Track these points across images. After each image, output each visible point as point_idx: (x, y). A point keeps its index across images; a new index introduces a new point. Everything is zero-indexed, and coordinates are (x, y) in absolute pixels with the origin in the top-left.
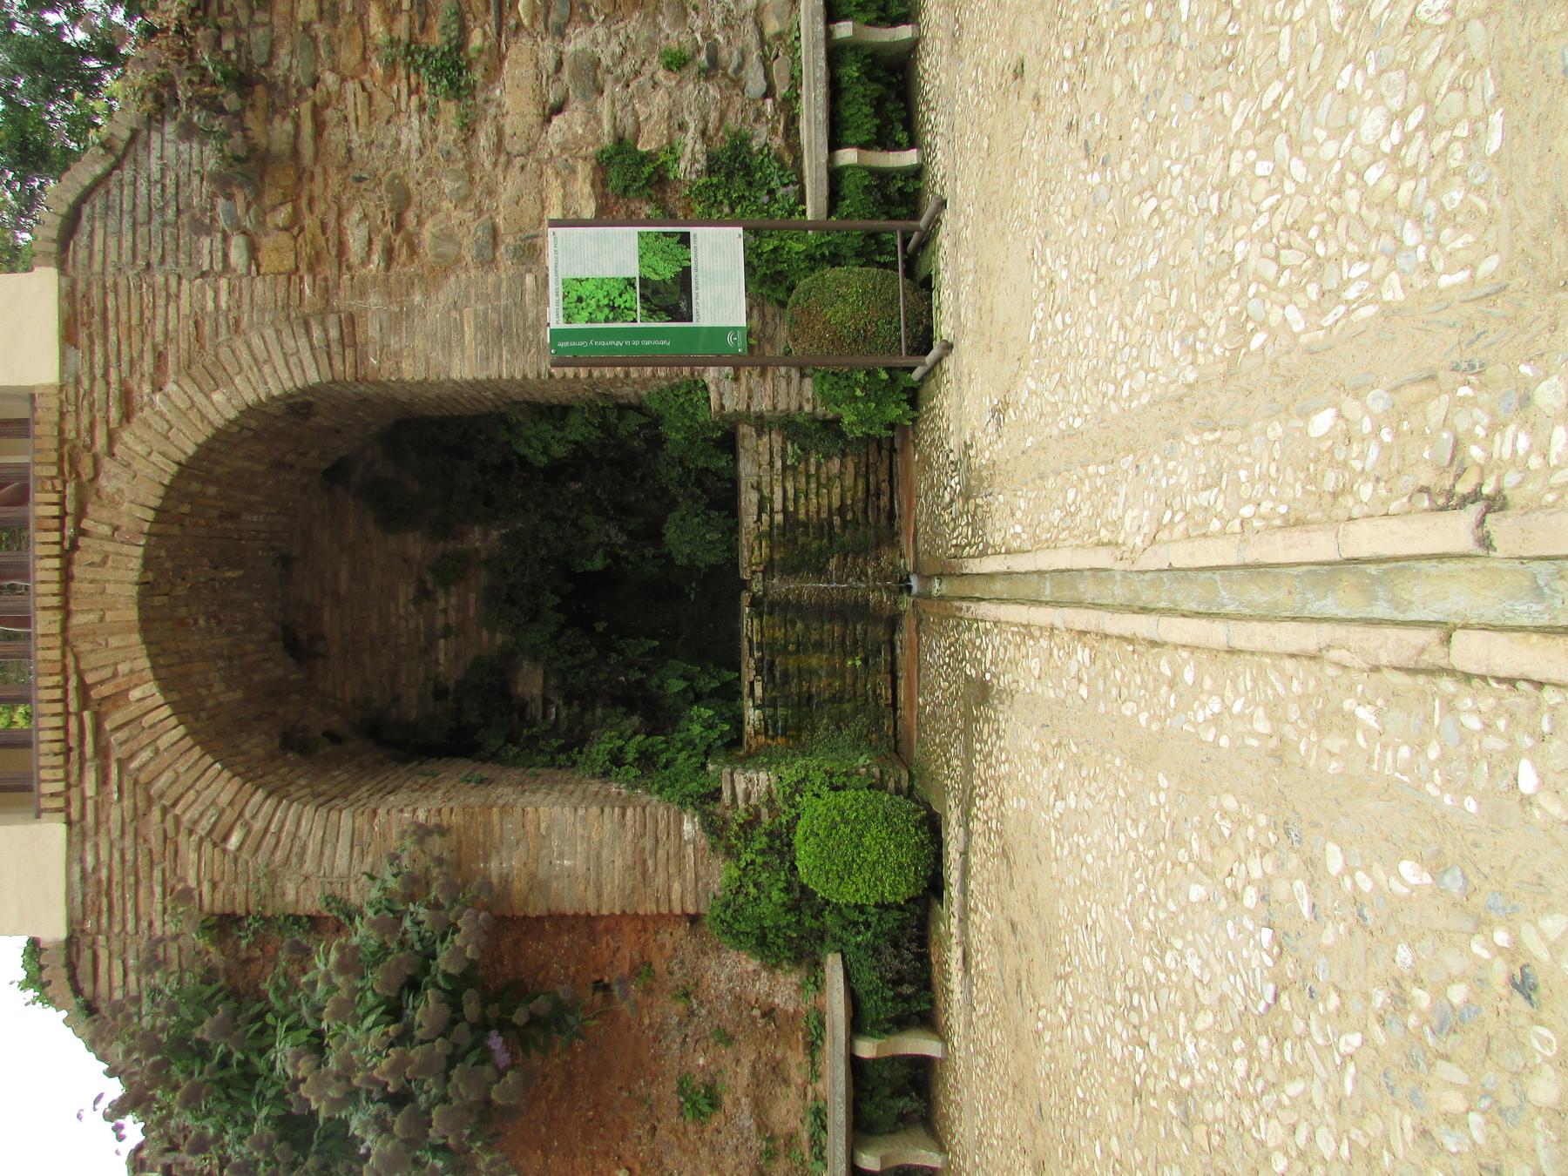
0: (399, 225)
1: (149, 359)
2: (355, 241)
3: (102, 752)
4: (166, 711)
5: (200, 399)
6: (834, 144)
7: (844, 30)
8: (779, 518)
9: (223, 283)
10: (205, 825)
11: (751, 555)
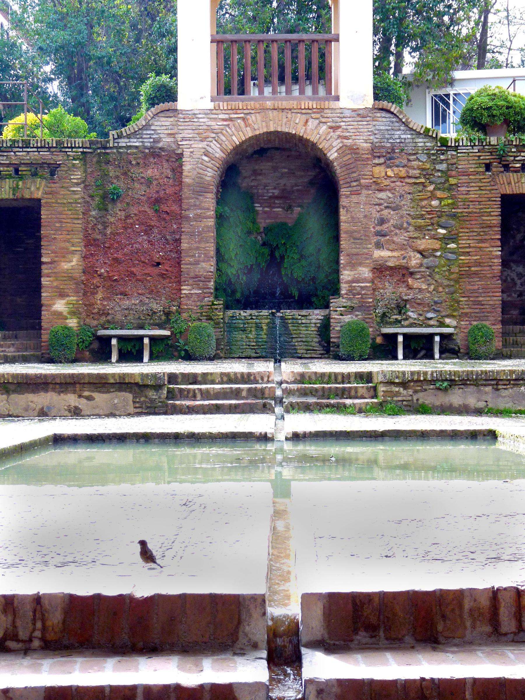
0: (386, 207)
1: (348, 134)
2: (382, 195)
3: (231, 119)
4: (244, 139)
5: (335, 149)
6: (405, 335)
7: (437, 339)
8: (300, 322)
9: (370, 156)
10: (210, 149)
11: (288, 313)
